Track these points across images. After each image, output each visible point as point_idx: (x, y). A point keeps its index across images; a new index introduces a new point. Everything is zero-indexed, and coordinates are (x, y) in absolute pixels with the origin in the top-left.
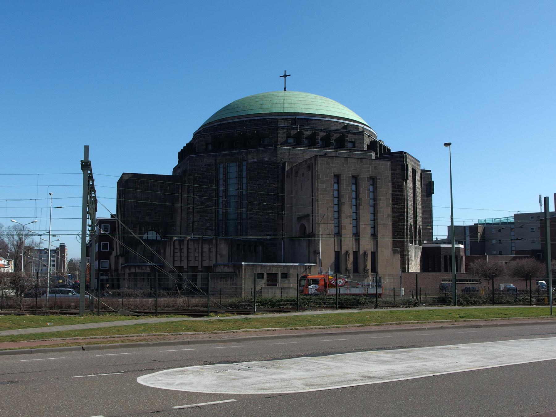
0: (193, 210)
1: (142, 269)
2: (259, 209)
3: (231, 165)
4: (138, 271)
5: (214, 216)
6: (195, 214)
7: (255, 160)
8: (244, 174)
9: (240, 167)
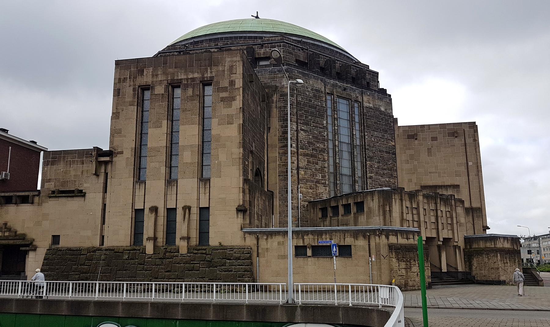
0: (298, 150)
1: (407, 239)
2: (378, 167)
3: (341, 101)
4: (402, 241)
5: (326, 165)
6: (300, 157)
7: (371, 105)
8: (357, 119)
9: (353, 107)
